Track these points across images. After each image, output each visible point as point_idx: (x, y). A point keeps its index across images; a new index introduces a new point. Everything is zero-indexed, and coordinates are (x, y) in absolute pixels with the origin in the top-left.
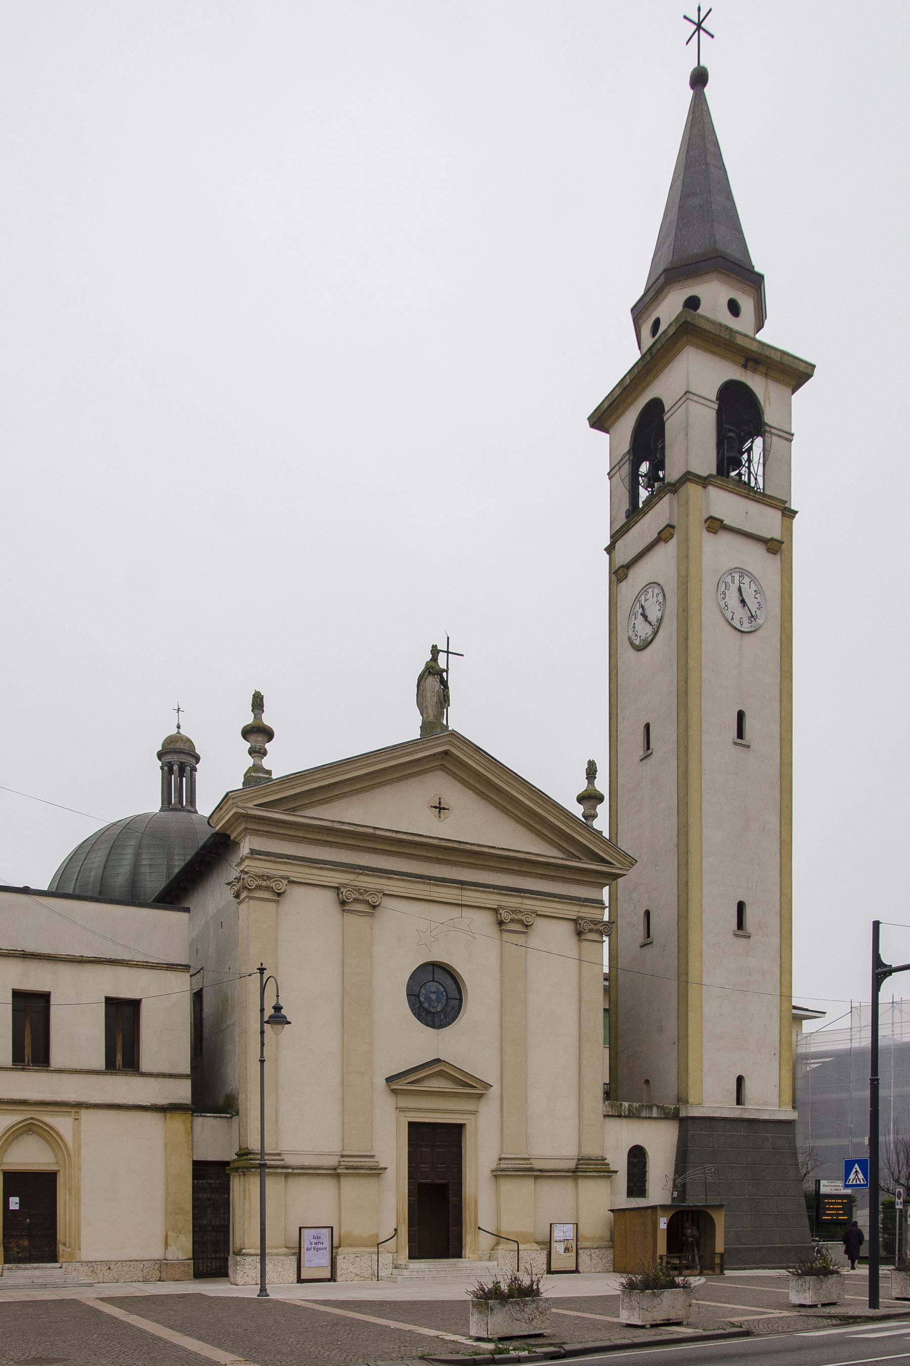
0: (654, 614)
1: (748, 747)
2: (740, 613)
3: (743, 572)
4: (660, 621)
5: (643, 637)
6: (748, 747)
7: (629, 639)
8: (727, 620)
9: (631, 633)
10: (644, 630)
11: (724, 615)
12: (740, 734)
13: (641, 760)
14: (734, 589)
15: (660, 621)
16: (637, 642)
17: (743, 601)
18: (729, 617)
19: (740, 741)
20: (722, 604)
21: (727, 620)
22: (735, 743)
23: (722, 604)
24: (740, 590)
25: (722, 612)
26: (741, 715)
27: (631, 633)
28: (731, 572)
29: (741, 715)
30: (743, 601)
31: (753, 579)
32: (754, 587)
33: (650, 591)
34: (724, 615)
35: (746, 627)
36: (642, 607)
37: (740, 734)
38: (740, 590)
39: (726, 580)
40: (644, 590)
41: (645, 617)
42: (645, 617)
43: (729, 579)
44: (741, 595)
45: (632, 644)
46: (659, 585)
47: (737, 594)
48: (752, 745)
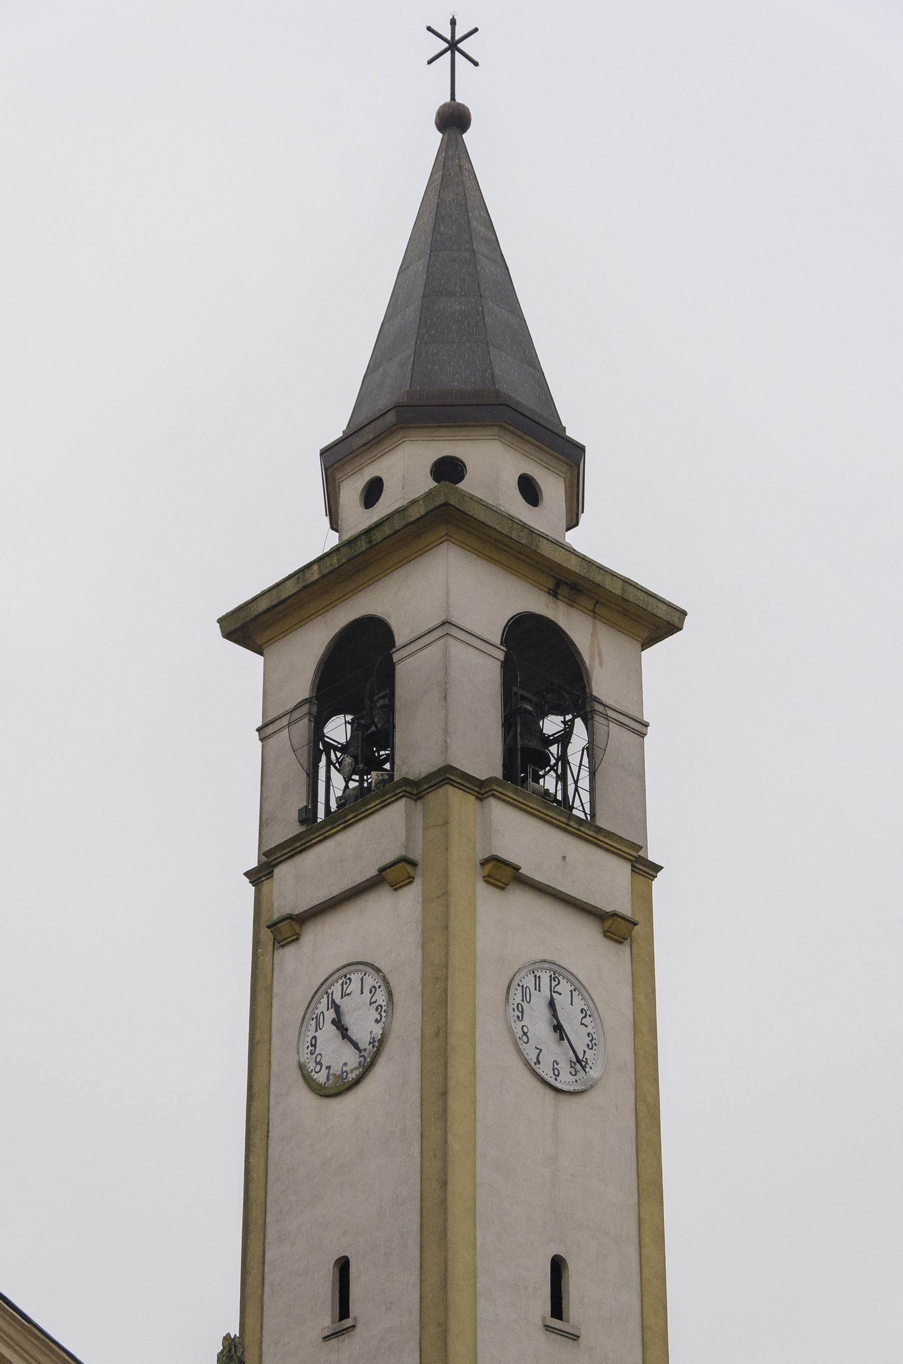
0: (364, 1026)
1: (575, 1338)
2: (553, 1053)
3: (557, 972)
4: (379, 1044)
5: (336, 1069)
6: (575, 1338)
7: (301, 1067)
8: (527, 1063)
9: (305, 1056)
10: (339, 1057)
11: (520, 1053)
12: (557, 1309)
13: (326, 1338)
14: (539, 1001)
15: (379, 1044)
16: (321, 1077)
17: (558, 1028)
18: (532, 1057)
19: (556, 1323)
20: (517, 1027)
21: (527, 1063)
22: (547, 1327)
23: (517, 1027)
24: (552, 1004)
25: (516, 1045)
26: (558, 1266)
27: (305, 1056)
28: (535, 966)
29: (558, 1266)
30: (558, 1028)
31: (578, 987)
32: (579, 1003)
33: (355, 977)
34: (520, 1053)
35: (565, 1081)
36: (337, 1008)
37: (557, 1309)
38: (552, 1004)
39: (525, 983)
40: (344, 972)
41: (339, 1024)
42: (339, 1024)
43: (529, 982)
44: (555, 1015)
45: (307, 1078)
46: (378, 970)
47: (546, 1013)
48: (583, 1332)
